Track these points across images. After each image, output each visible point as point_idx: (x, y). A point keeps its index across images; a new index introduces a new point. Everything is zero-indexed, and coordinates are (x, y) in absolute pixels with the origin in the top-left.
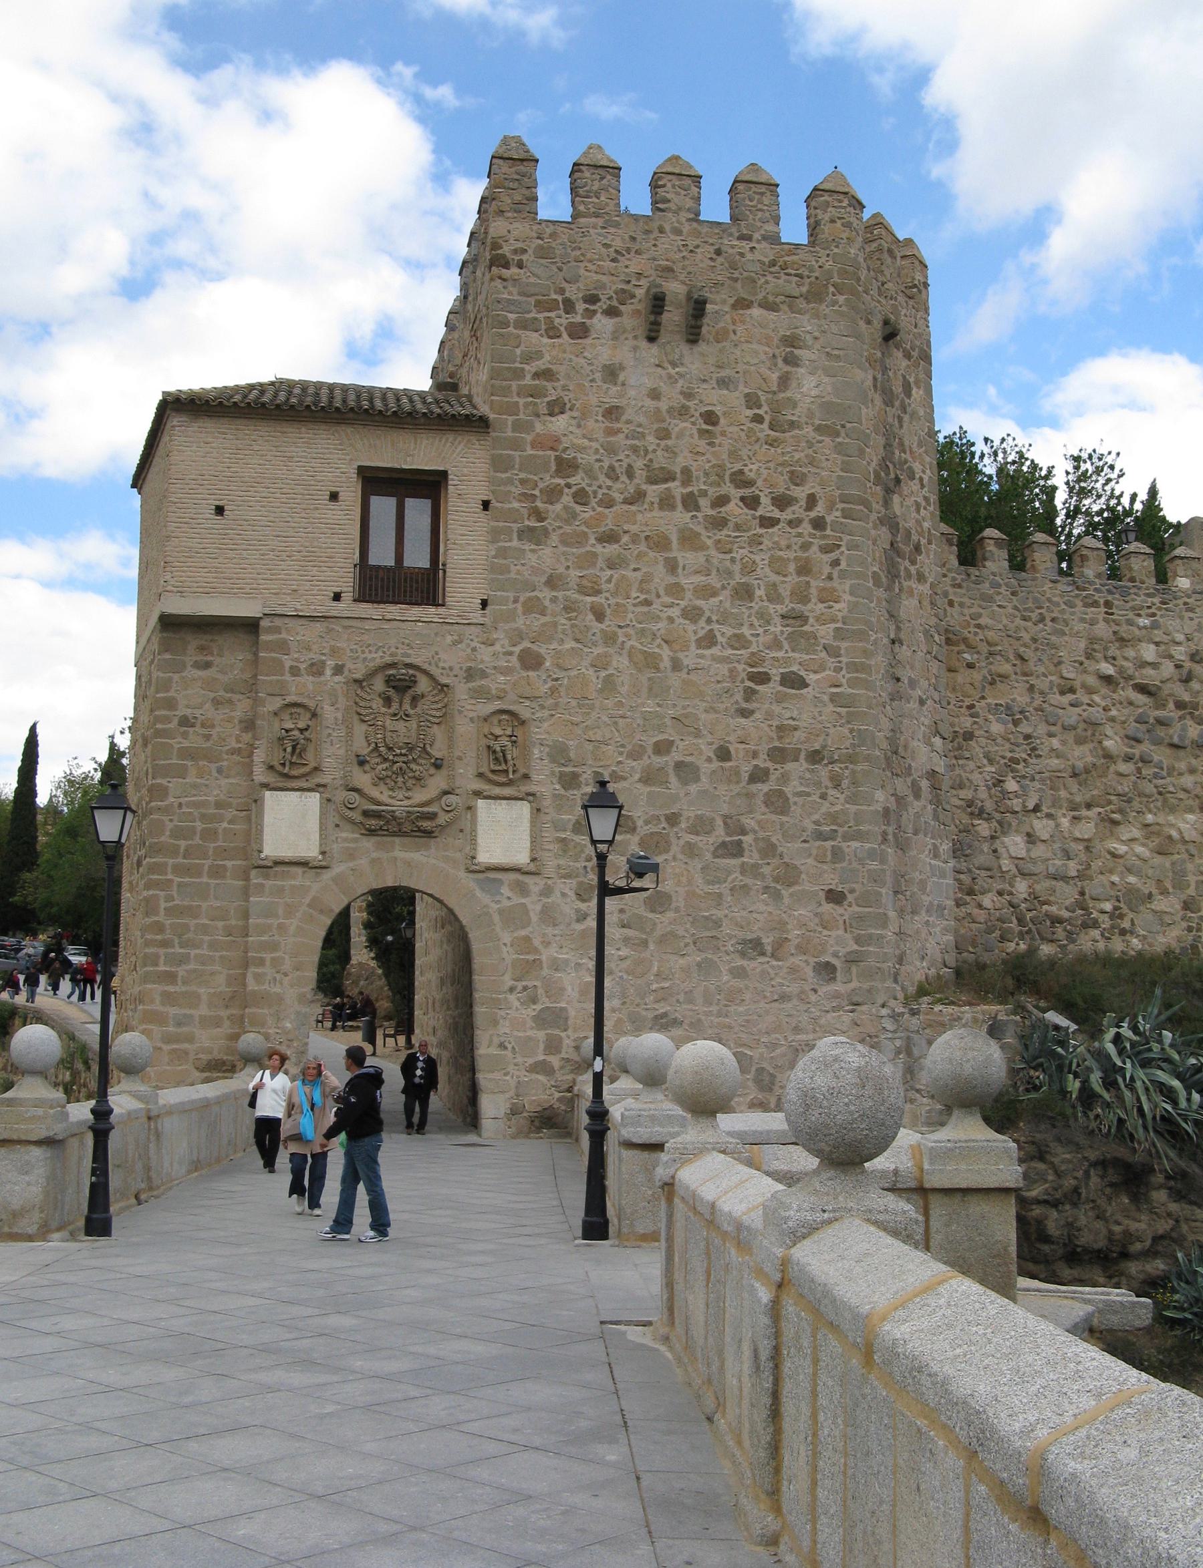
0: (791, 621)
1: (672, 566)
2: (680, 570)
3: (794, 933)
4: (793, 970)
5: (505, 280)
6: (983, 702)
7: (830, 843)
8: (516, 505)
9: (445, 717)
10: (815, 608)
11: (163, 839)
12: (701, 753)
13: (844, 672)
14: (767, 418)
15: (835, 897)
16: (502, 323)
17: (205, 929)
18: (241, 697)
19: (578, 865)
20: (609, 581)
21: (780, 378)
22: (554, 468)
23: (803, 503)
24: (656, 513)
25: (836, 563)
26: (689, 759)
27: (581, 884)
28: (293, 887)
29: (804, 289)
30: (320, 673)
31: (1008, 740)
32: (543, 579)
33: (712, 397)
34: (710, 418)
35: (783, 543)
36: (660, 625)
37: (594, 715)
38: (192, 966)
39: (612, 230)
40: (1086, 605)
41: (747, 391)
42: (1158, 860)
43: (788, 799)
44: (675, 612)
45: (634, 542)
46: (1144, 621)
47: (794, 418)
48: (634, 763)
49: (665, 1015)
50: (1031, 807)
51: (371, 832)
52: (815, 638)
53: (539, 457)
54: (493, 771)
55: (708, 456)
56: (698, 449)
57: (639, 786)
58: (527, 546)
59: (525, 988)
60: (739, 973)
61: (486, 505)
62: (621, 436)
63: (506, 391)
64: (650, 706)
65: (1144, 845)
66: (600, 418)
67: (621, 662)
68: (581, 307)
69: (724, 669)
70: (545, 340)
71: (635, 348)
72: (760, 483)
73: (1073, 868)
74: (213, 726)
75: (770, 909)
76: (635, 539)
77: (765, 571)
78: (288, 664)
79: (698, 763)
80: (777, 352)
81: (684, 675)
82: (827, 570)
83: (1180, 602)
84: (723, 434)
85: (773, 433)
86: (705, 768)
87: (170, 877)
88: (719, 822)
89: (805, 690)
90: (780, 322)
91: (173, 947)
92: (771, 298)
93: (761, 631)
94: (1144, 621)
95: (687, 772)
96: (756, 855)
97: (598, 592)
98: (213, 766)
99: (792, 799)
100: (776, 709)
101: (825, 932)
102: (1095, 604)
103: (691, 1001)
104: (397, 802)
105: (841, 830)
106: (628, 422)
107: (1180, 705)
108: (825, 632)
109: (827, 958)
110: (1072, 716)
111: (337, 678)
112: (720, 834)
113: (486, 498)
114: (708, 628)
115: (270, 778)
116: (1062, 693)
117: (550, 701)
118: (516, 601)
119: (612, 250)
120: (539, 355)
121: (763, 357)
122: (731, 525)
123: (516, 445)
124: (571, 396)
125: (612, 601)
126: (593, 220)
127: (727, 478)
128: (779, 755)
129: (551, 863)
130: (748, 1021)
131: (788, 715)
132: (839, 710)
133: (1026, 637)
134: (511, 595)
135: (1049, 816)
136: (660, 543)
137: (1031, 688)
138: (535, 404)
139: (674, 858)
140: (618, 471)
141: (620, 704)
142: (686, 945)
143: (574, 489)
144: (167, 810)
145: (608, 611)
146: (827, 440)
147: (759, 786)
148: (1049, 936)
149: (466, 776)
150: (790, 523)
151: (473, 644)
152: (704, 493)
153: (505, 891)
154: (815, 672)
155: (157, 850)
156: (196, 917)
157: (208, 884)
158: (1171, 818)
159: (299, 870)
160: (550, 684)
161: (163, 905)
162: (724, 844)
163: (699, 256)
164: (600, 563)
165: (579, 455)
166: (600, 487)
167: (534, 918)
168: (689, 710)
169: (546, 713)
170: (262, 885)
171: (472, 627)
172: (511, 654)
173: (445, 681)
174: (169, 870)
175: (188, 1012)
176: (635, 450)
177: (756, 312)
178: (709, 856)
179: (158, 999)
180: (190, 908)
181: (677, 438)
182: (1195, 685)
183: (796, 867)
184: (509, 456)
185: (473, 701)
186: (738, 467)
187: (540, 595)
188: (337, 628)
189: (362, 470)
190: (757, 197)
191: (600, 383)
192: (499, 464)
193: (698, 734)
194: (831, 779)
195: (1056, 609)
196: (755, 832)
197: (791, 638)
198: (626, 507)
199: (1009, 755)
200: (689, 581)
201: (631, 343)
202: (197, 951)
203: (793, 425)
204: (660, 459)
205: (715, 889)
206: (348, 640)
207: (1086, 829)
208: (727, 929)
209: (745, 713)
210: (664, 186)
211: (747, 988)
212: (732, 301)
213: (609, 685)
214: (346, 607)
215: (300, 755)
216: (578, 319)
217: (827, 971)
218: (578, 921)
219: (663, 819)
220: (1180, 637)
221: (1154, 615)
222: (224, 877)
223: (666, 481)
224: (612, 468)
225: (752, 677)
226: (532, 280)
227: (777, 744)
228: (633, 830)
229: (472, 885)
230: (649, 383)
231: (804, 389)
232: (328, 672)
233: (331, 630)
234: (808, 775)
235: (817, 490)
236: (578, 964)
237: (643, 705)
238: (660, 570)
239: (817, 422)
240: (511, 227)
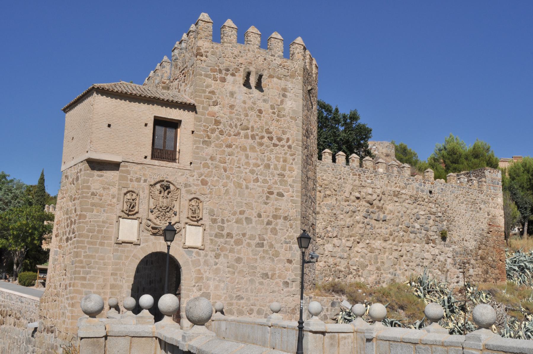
0: (280, 176)
1: (247, 157)
2: (249, 158)
3: (277, 272)
4: (277, 283)
5: (202, 61)
6: (323, 203)
7: (288, 245)
8: (202, 133)
10: (287, 173)
11: (84, 232)
12: (253, 215)
13: (295, 193)
14: (277, 113)
15: (290, 261)
16: (200, 74)
17: (96, 263)
18: (112, 187)
19: (215, 247)
20: (229, 159)
21: (281, 101)
22: (214, 122)
23: (285, 140)
24: (243, 139)
25: (294, 159)
26: (249, 216)
27: (216, 254)
28: (127, 250)
29: (289, 74)
30: (139, 181)
31: (329, 215)
32: (209, 157)
33: (261, 105)
34: (260, 111)
35: (279, 152)
36: (243, 174)
37: (222, 201)
38: (92, 275)
39: (234, 48)
40: (353, 175)
41: (271, 104)
42: (369, 254)
43: (277, 231)
44: (247, 171)
45: (236, 148)
46: (369, 181)
47: (284, 114)
48: (233, 217)
49: (239, 296)
50: (335, 236)
51: (154, 234)
52: (287, 182)
53: (209, 118)
54: (192, 217)
55: (259, 123)
56: (256, 121)
57: (235, 224)
58: (205, 147)
59: (198, 286)
60: (261, 283)
61: (193, 132)
62: (234, 114)
63: (200, 96)
64: (239, 199)
65: (366, 250)
66: (228, 108)
67: (231, 185)
68: (224, 72)
69: (261, 190)
70: (213, 81)
71: (239, 87)
72: (273, 133)
73: (345, 255)
74: (103, 196)
75: (270, 264)
76: (237, 147)
77: (273, 160)
78: (129, 178)
79: (252, 218)
80: (280, 93)
81: (249, 190)
82: (291, 161)
83: (380, 176)
84: (264, 117)
85: (277, 118)
86: (254, 220)
87: (86, 245)
88: (257, 237)
89: (283, 198)
90: (282, 83)
91: (86, 268)
92: (279, 76)
93: (272, 178)
94: (369, 181)
96: (268, 247)
97: (225, 163)
98: (102, 209)
99: (279, 231)
100: (275, 203)
101: (286, 272)
102: (356, 175)
103: (246, 292)
105: (292, 241)
106: (237, 110)
107: (378, 207)
108: (290, 180)
109: (286, 280)
110: (347, 209)
111: (144, 184)
112: (257, 240)
113: (193, 130)
114: (257, 176)
115: (123, 214)
116: (346, 201)
117: (209, 196)
118: (201, 163)
119: (234, 55)
120: (211, 86)
121: (276, 94)
122: (265, 145)
123: (203, 114)
124: (220, 100)
125: (229, 166)
126: (229, 44)
127: (264, 131)
128: (275, 217)
129: (208, 246)
130: (263, 298)
131: (278, 205)
132: (292, 204)
133: (336, 184)
134: (199, 161)
135: (340, 239)
136: (244, 149)
137: (337, 199)
138: (209, 102)
139: (244, 247)
140: (233, 125)
141: (230, 198)
142: (246, 274)
143: (219, 129)
144: (86, 223)
145: (228, 169)
146: (293, 121)
147: (269, 226)
148: (338, 276)
150: (281, 146)
151: (187, 176)
152: (257, 135)
153: (194, 254)
154: (287, 192)
155: (80, 236)
156: (94, 259)
157: (99, 248)
158: (374, 242)
159: (130, 245)
160: (210, 190)
161: (83, 254)
162: (258, 243)
163: (259, 60)
164: (226, 154)
165: (221, 119)
166: (227, 130)
167: (202, 264)
168: (250, 201)
169: (207, 199)
170: (118, 249)
171: (187, 171)
172: (198, 180)
173: (178, 187)
174: (86, 243)
175: (89, 290)
176: (238, 119)
177: (275, 79)
178: (254, 247)
179: (80, 286)
180: (92, 256)
181: (250, 116)
182: (382, 202)
183: (279, 252)
184: (200, 117)
185: (186, 194)
186: (267, 127)
187: (208, 162)
188: (146, 167)
190: (277, 43)
191: (228, 97)
193: (252, 210)
194: (290, 225)
195: (345, 176)
196: (267, 240)
197: (280, 181)
198: (235, 137)
199: (329, 219)
200: (252, 161)
201: (238, 85)
202: (94, 270)
203: (284, 116)
204: (245, 123)
205: (255, 257)
206: (149, 172)
207: (349, 244)
208: (258, 270)
209: (266, 203)
210: (250, 36)
211: (263, 288)
212: (268, 75)
214: (149, 160)
215: (132, 208)
216: (223, 76)
217: (286, 284)
218: (215, 265)
219: (241, 234)
220: (379, 187)
221: (372, 179)
222: (104, 246)
223: (247, 129)
224: (231, 124)
225: (269, 193)
226: (210, 61)
227: (275, 213)
228: (232, 237)
229: (184, 252)
230: (243, 98)
231: (287, 105)
232: (142, 181)
233: (143, 168)
234: (283, 224)
235: (290, 136)
236: (214, 279)
237: (237, 199)
238: (243, 158)
239: (291, 116)
240: (204, 44)
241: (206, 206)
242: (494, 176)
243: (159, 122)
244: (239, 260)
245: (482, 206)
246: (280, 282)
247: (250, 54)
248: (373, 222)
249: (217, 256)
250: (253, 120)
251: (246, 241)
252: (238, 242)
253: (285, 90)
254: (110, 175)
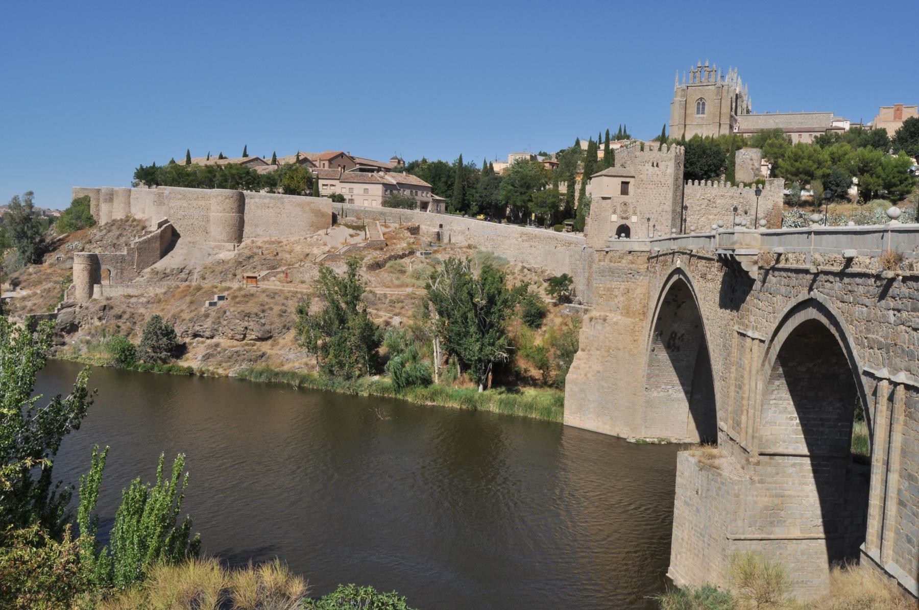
33: (658, 173)
67: (647, 202)
95: (653, 213)
104: (624, 216)
108: (668, 199)
112: (656, 219)
128: (662, 211)
149: (631, 213)
200: (654, 193)
217: (666, 234)
241: (638, 209)
242: (779, 183)
243: (623, 183)
245: (770, 198)
246: (664, 233)
247: (654, 155)
248: (711, 209)
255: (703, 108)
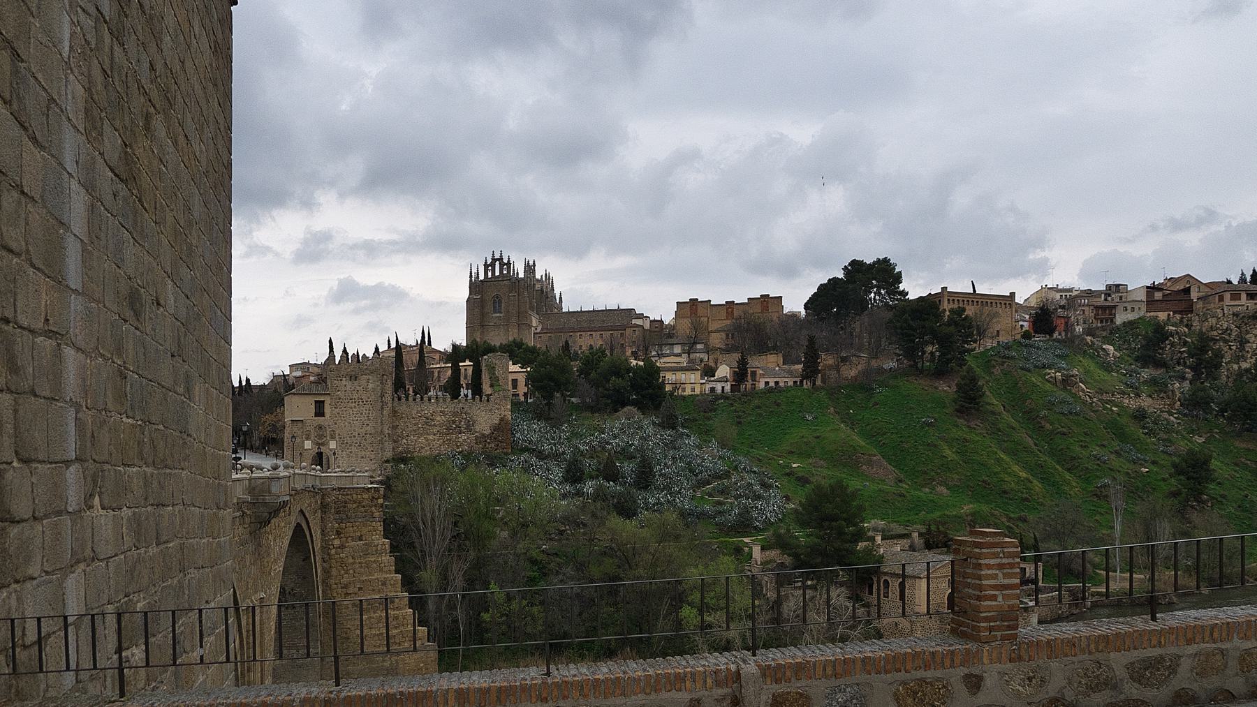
9: (326, 431)
15: (372, 451)
33: (358, 388)
90: (367, 377)
95: (354, 436)
104: (320, 442)
189: (315, 401)
192: (332, 399)
207: (415, 438)
213: (345, 426)
244: (351, 452)
249: (342, 451)
250: (355, 396)
251: (354, 444)
252: (350, 445)
253: (369, 379)
254: (300, 425)
255: (500, 306)
